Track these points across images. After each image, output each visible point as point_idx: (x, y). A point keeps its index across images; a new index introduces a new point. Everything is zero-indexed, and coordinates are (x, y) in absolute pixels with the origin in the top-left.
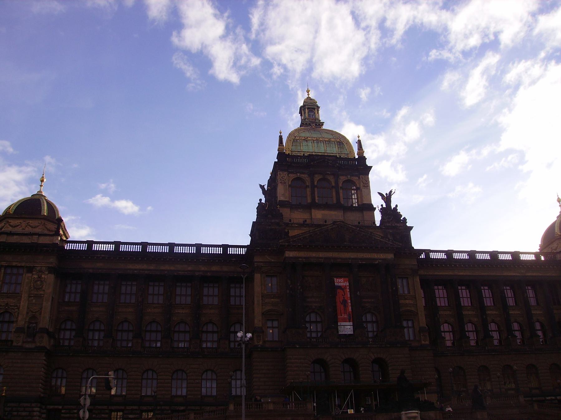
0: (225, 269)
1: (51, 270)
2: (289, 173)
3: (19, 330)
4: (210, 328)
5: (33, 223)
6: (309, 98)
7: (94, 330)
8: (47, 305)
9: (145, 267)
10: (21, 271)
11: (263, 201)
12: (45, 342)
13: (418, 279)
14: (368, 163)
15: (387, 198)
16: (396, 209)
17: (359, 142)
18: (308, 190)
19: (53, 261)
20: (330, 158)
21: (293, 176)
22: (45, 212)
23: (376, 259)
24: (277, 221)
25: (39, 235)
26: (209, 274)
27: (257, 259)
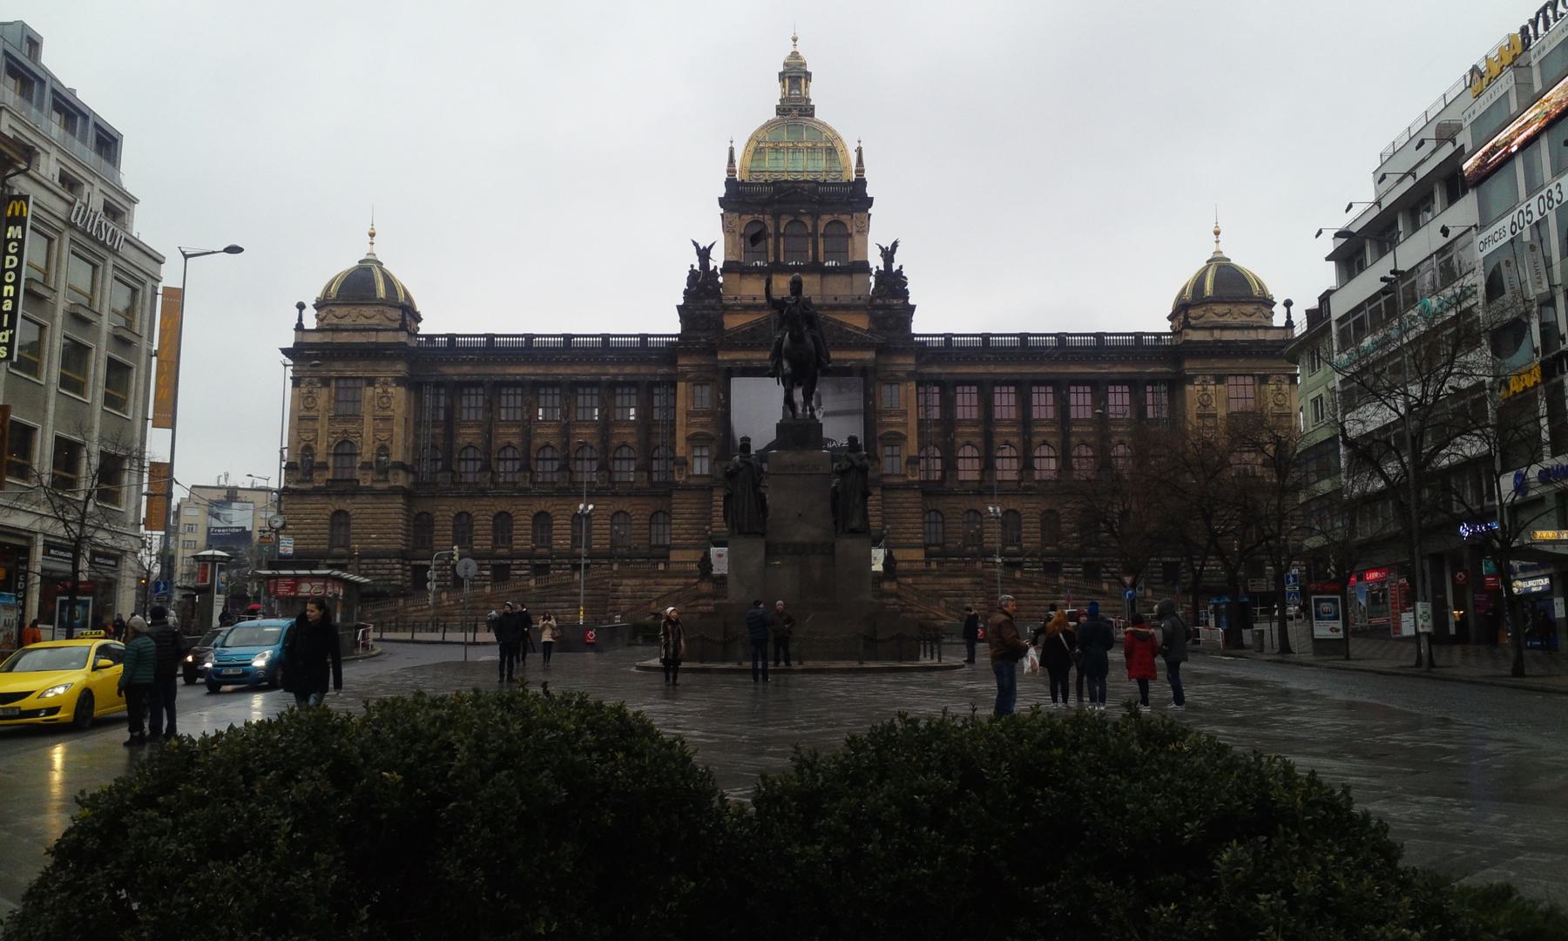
0: (643, 370)
1: (399, 381)
2: (742, 213)
3: (366, 466)
4: (625, 452)
5: (367, 311)
6: (795, 55)
7: (466, 460)
8: (399, 431)
9: (531, 370)
10: (358, 383)
11: (697, 267)
12: (401, 480)
13: (912, 386)
14: (870, 192)
15: (888, 255)
16: (900, 271)
17: (859, 151)
18: (771, 241)
19: (401, 368)
20: (806, 186)
21: (748, 218)
22: (381, 291)
23: (846, 361)
24: (713, 301)
25: (377, 330)
26: (621, 379)
27: (680, 362)
